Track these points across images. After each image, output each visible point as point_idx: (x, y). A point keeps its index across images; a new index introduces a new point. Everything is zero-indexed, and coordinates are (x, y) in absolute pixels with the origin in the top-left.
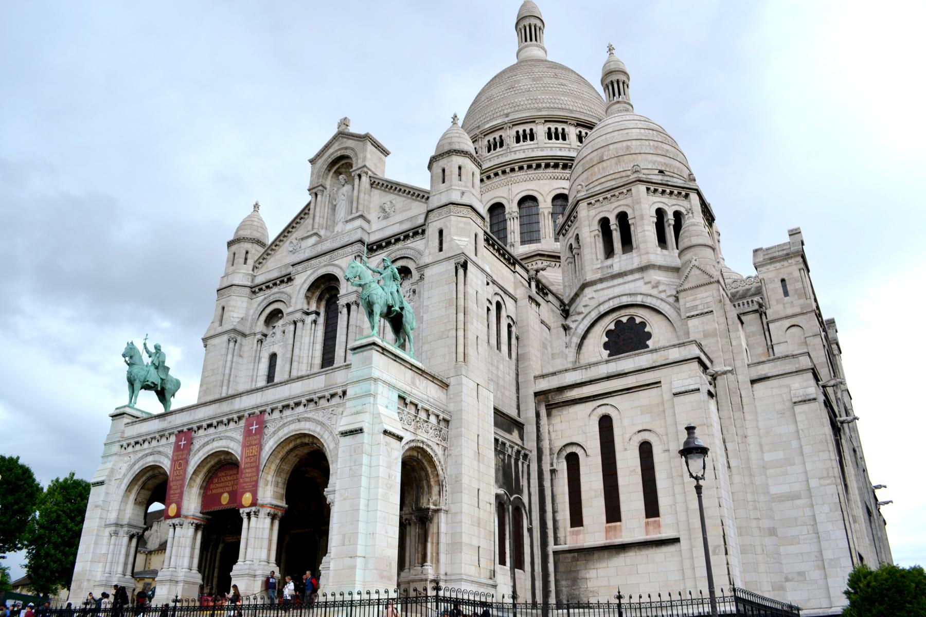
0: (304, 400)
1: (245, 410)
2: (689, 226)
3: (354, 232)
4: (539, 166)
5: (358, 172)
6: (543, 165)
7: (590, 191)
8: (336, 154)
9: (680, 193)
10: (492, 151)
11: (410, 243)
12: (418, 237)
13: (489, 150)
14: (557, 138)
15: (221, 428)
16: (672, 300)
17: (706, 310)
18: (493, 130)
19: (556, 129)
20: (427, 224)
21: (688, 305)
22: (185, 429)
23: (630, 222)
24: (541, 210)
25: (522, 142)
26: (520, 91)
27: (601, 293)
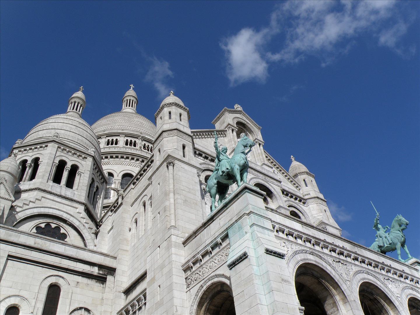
5: (260, 142)
8: (242, 120)
20: (308, 201)
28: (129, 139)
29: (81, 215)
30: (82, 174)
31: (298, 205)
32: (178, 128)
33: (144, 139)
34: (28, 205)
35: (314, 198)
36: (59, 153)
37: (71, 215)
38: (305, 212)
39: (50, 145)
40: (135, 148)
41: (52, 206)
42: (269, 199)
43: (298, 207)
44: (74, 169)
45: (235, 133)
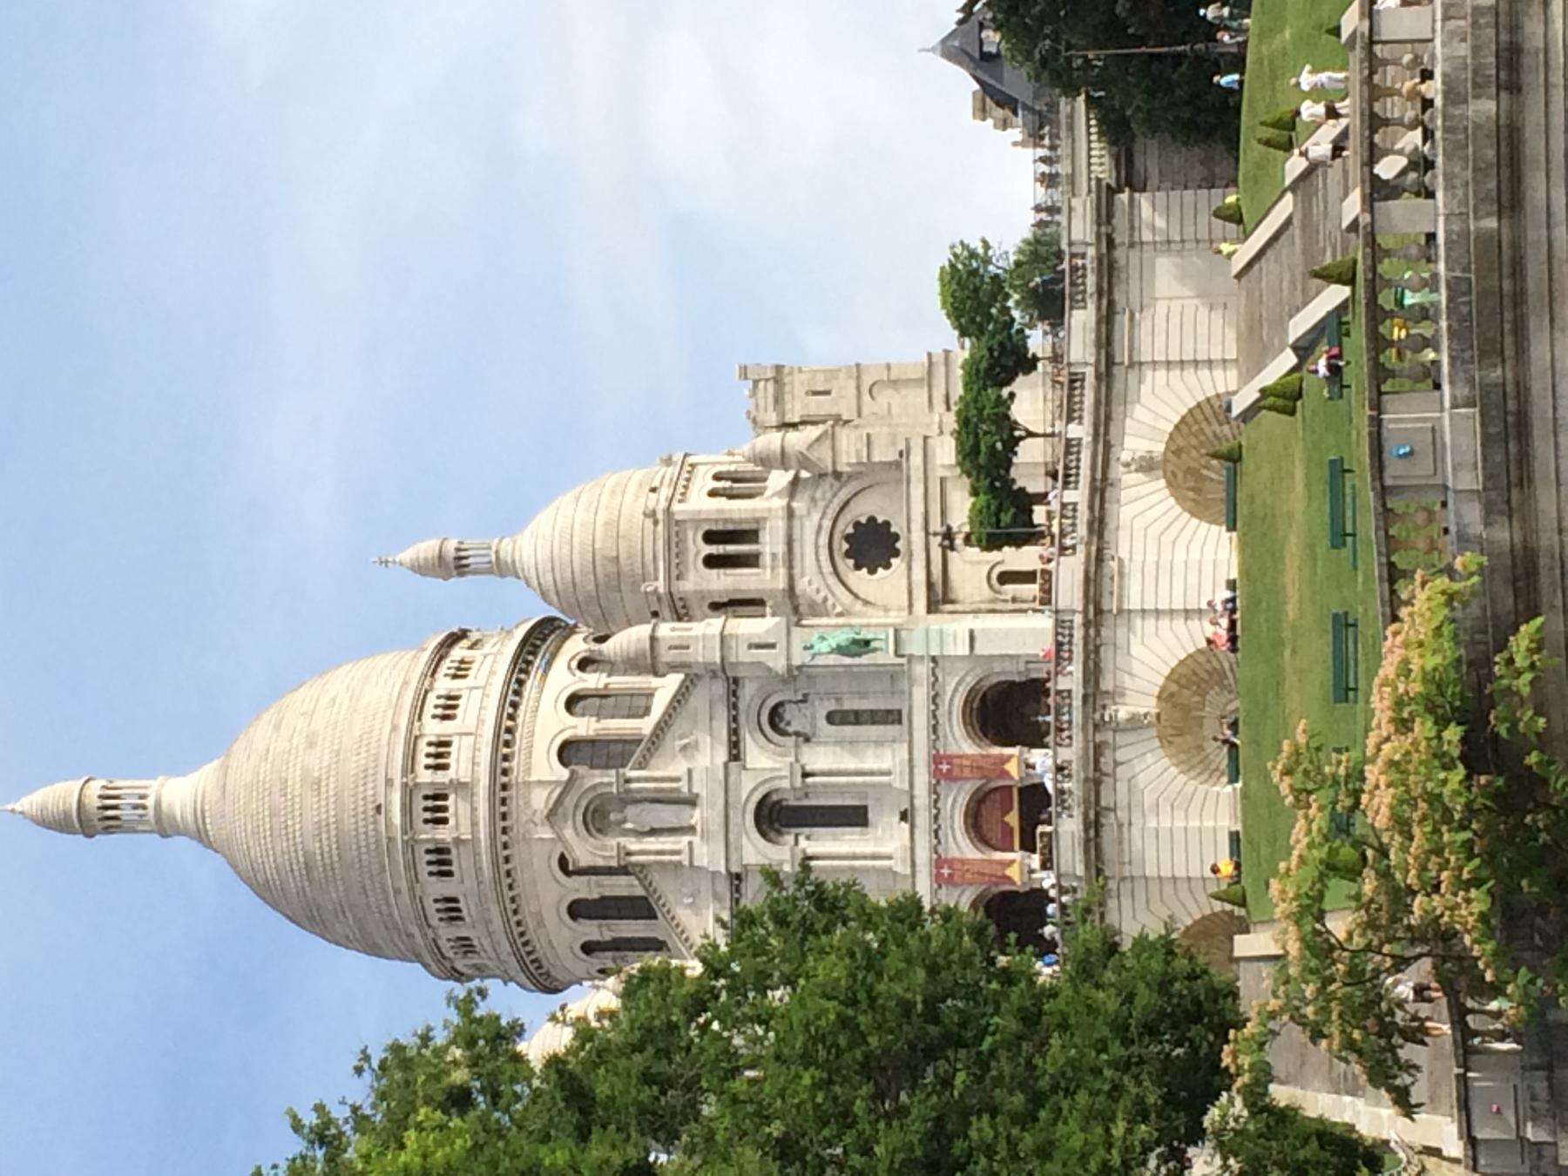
4: (509, 730)
6: (510, 723)
11: (742, 705)
12: (739, 693)
13: (444, 821)
14: (454, 707)
15: (941, 821)
16: (837, 485)
18: (407, 809)
19: (436, 707)
20: (730, 674)
21: (854, 460)
23: (721, 527)
24: (591, 733)
25: (451, 761)
27: (807, 571)
38: (758, 690)
42: (775, 798)
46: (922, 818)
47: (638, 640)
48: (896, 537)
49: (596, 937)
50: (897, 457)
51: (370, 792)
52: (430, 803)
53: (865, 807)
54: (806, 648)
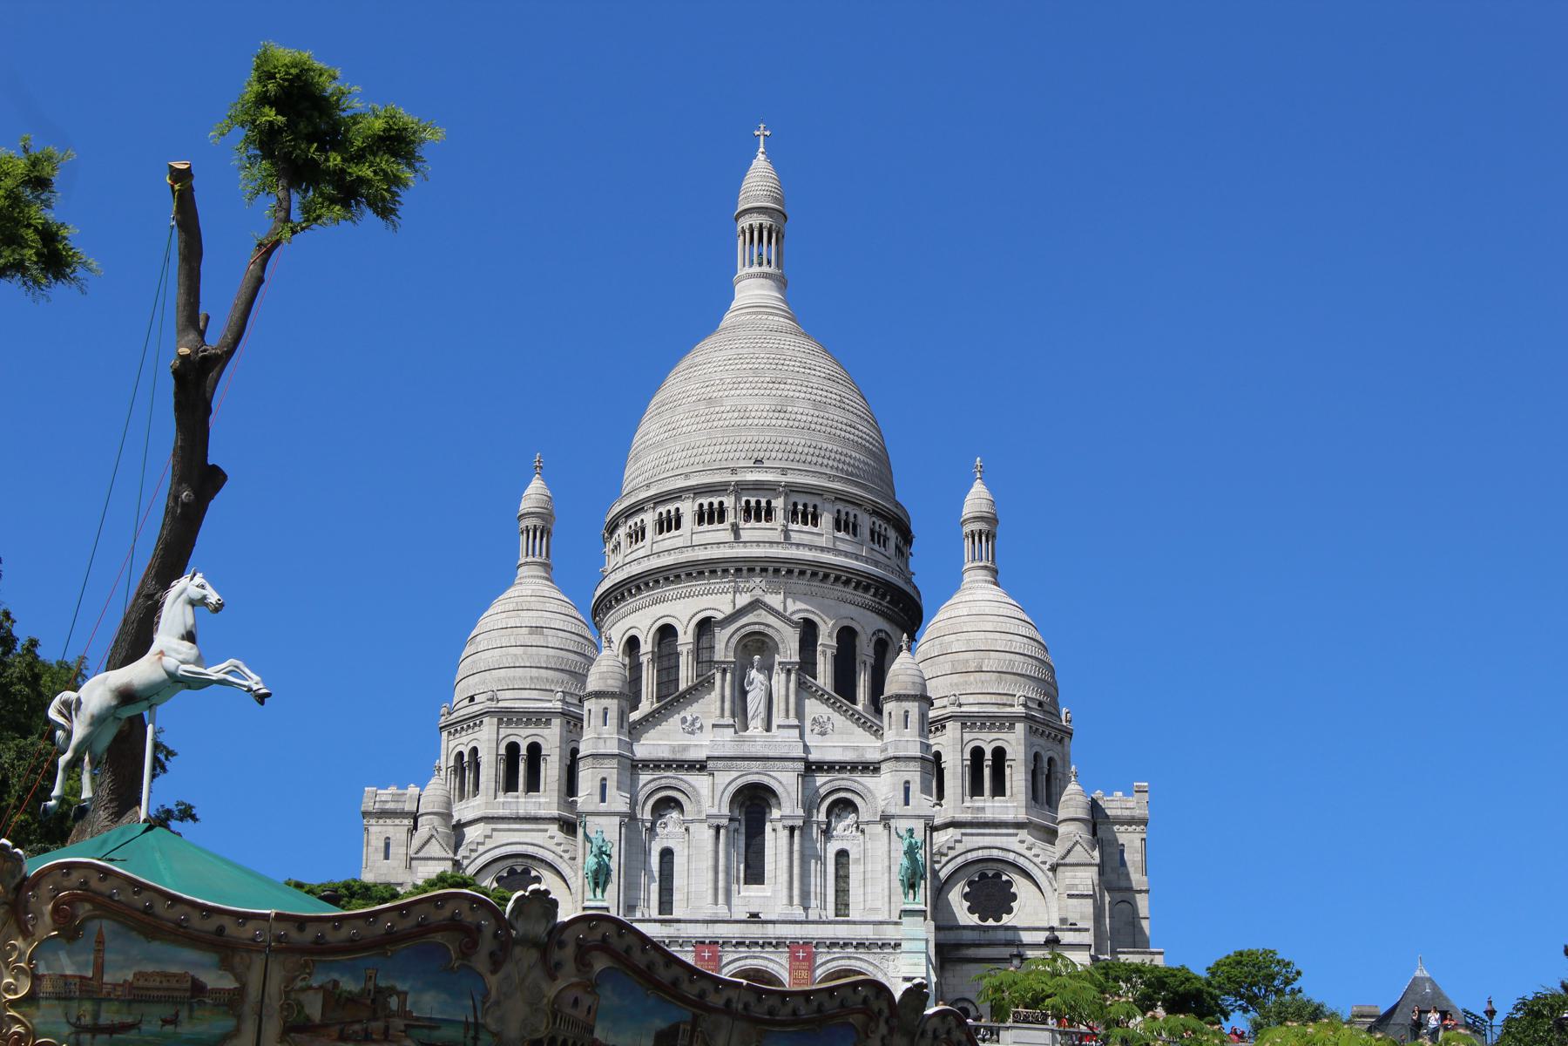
0: (854, 943)
1: (786, 938)
2: (1075, 794)
3: (794, 744)
4: (826, 576)
6: (832, 576)
7: (963, 709)
9: (1056, 736)
10: (753, 523)
17: (1086, 893)
18: (758, 487)
19: (847, 514)
20: (883, 766)
21: (1068, 881)
22: (707, 941)
26: (796, 424)
28: (705, 501)
29: (555, 840)
30: (548, 758)
31: (855, 781)
32: (594, 751)
33: (741, 488)
34: (476, 851)
35: (891, 758)
36: (503, 732)
37: (540, 846)
38: (870, 791)
39: (486, 720)
40: (721, 526)
41: (510, 841)
42: (773, 801)
43: (854, 786)
44: (535, 749)
45: (728, 676)
46: (754, 931)
47: (913, 683)
48: (998, 919)
49: (642, 652)
50: (1070, 921)
51: (774, 455)
52: (763, 504)
53: (763, 884)
54: (911, 831)
